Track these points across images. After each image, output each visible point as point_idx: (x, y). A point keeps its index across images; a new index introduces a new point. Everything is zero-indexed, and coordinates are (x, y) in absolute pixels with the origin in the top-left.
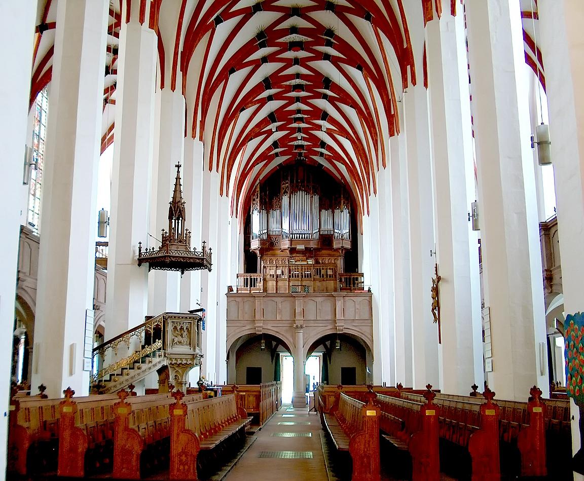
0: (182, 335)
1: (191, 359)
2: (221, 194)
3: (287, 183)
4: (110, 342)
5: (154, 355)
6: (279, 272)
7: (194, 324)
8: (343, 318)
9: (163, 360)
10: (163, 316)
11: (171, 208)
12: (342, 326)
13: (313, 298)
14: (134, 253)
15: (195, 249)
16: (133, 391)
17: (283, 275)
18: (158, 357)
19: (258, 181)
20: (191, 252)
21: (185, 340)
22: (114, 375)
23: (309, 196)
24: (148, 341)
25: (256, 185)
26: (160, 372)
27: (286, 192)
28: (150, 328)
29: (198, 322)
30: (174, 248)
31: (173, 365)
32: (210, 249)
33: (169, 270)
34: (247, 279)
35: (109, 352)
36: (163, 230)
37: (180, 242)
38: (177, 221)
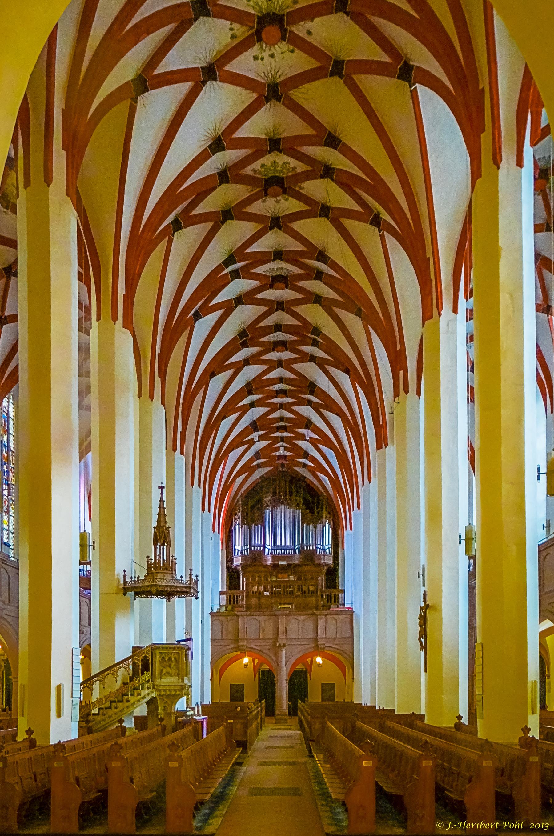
0: (170, 666)
1: (179, 690)
2: (203, 510)
3: (269, 496)
4: (97, 675)
5: (143, 688)
6: (262, 588)
7: (182, 654)
9: (152, 692)
10: (151, 647)
11: (155, 533)
14: (119, 580)
15: (181, 577)
16: (123, 725)
18: (146, 689)
19: (240, 494)
20: (177, 580)
21: (173, 671)
22: (102, 708)
24: (135, 674)
25: (238, 498)
26: (147, 703)
27: (268, 506)
28: (138, 660)
29: (186, 652)
30: (159, 576)
31: (162, 696)
32: (197, 576)
33: (155, 598)
34: (230, 596)
35: (96, 686)
36: (148, 557)
37: (167, 569)
38: (162, 547)
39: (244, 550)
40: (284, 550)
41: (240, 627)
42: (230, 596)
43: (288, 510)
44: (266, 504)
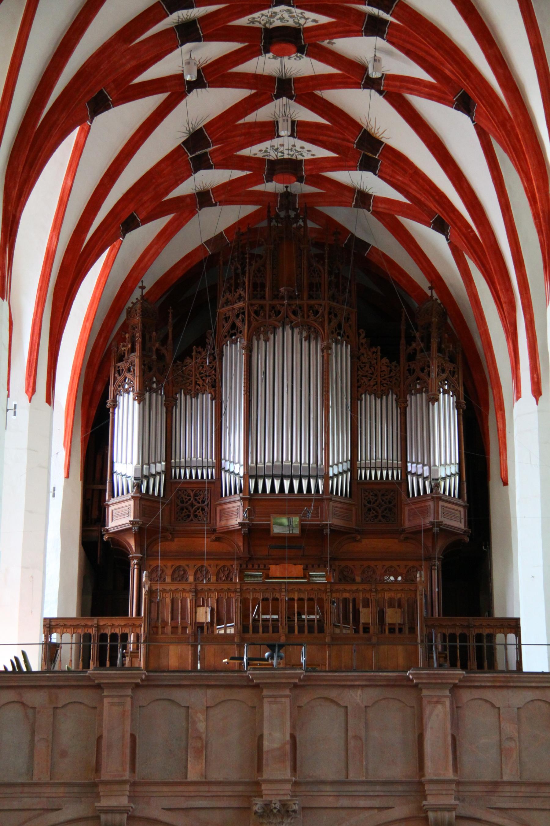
3: (240, 298)
8: (450, 775)
12: (450, 809)
13: (333, 694)
17: (220, 622)
19: (137, 294)
23: (316, 347)
39: (147, 478)
40: (291, 477)
41: (105, 734)
42: (87, 637)
43: (305, 344)
44: (227, 326)
